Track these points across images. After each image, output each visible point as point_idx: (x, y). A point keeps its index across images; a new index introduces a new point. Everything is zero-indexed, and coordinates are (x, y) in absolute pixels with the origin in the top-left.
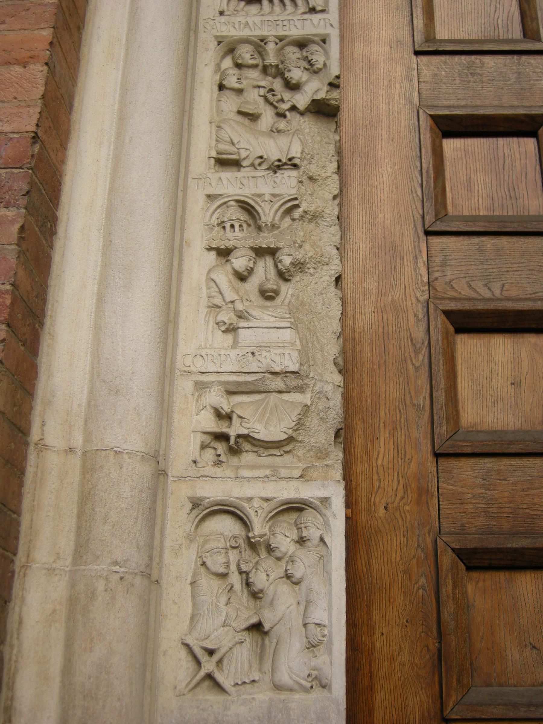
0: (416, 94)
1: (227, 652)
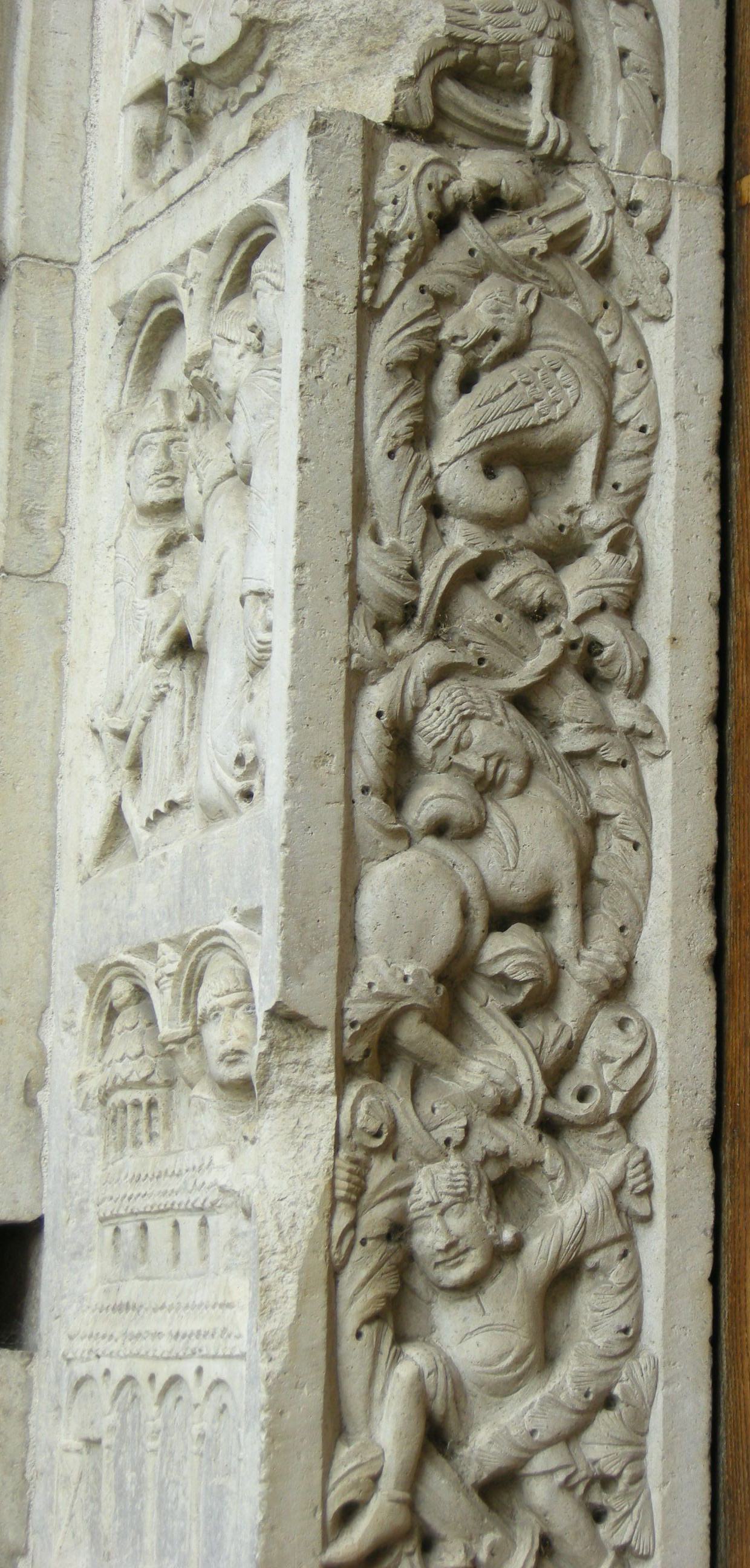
1: (142, 732)
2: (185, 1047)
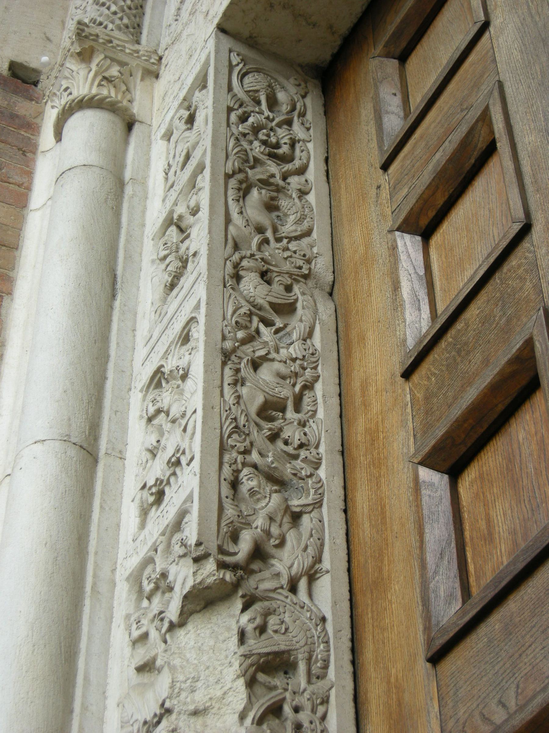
0: (412, 439)
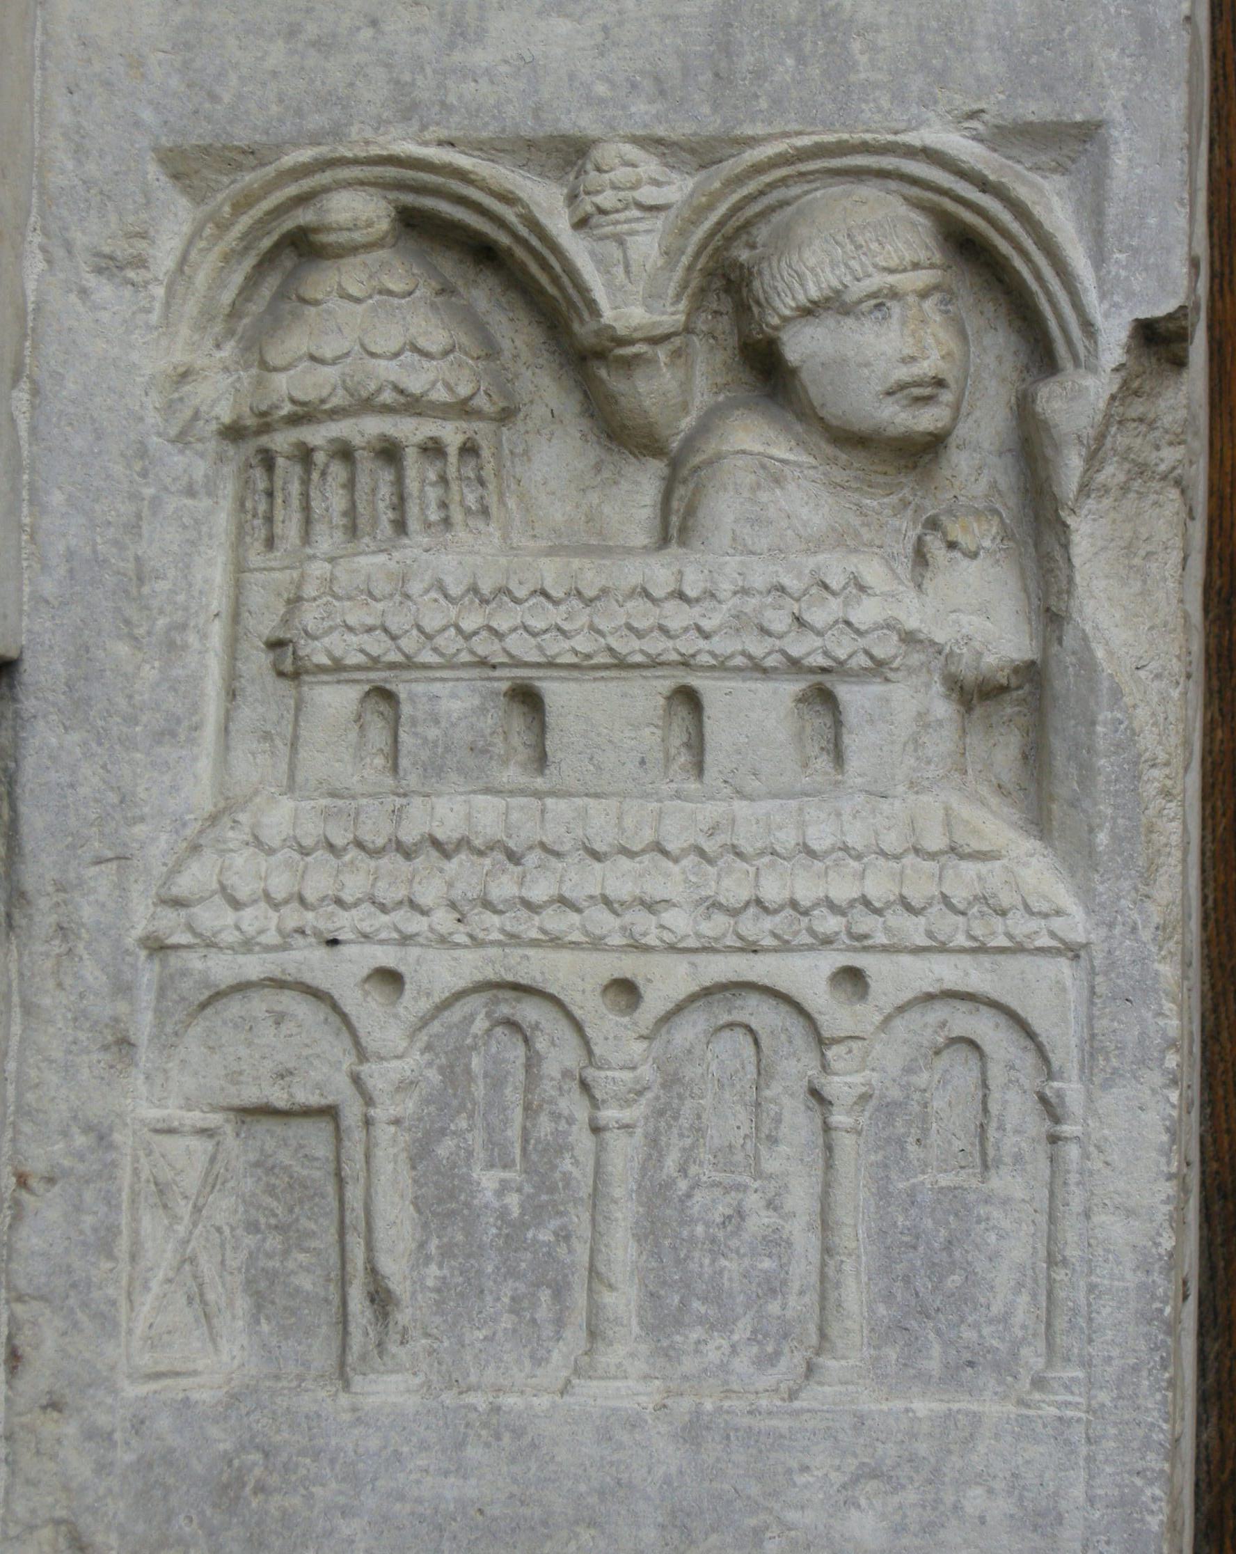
2: (662, 354)
